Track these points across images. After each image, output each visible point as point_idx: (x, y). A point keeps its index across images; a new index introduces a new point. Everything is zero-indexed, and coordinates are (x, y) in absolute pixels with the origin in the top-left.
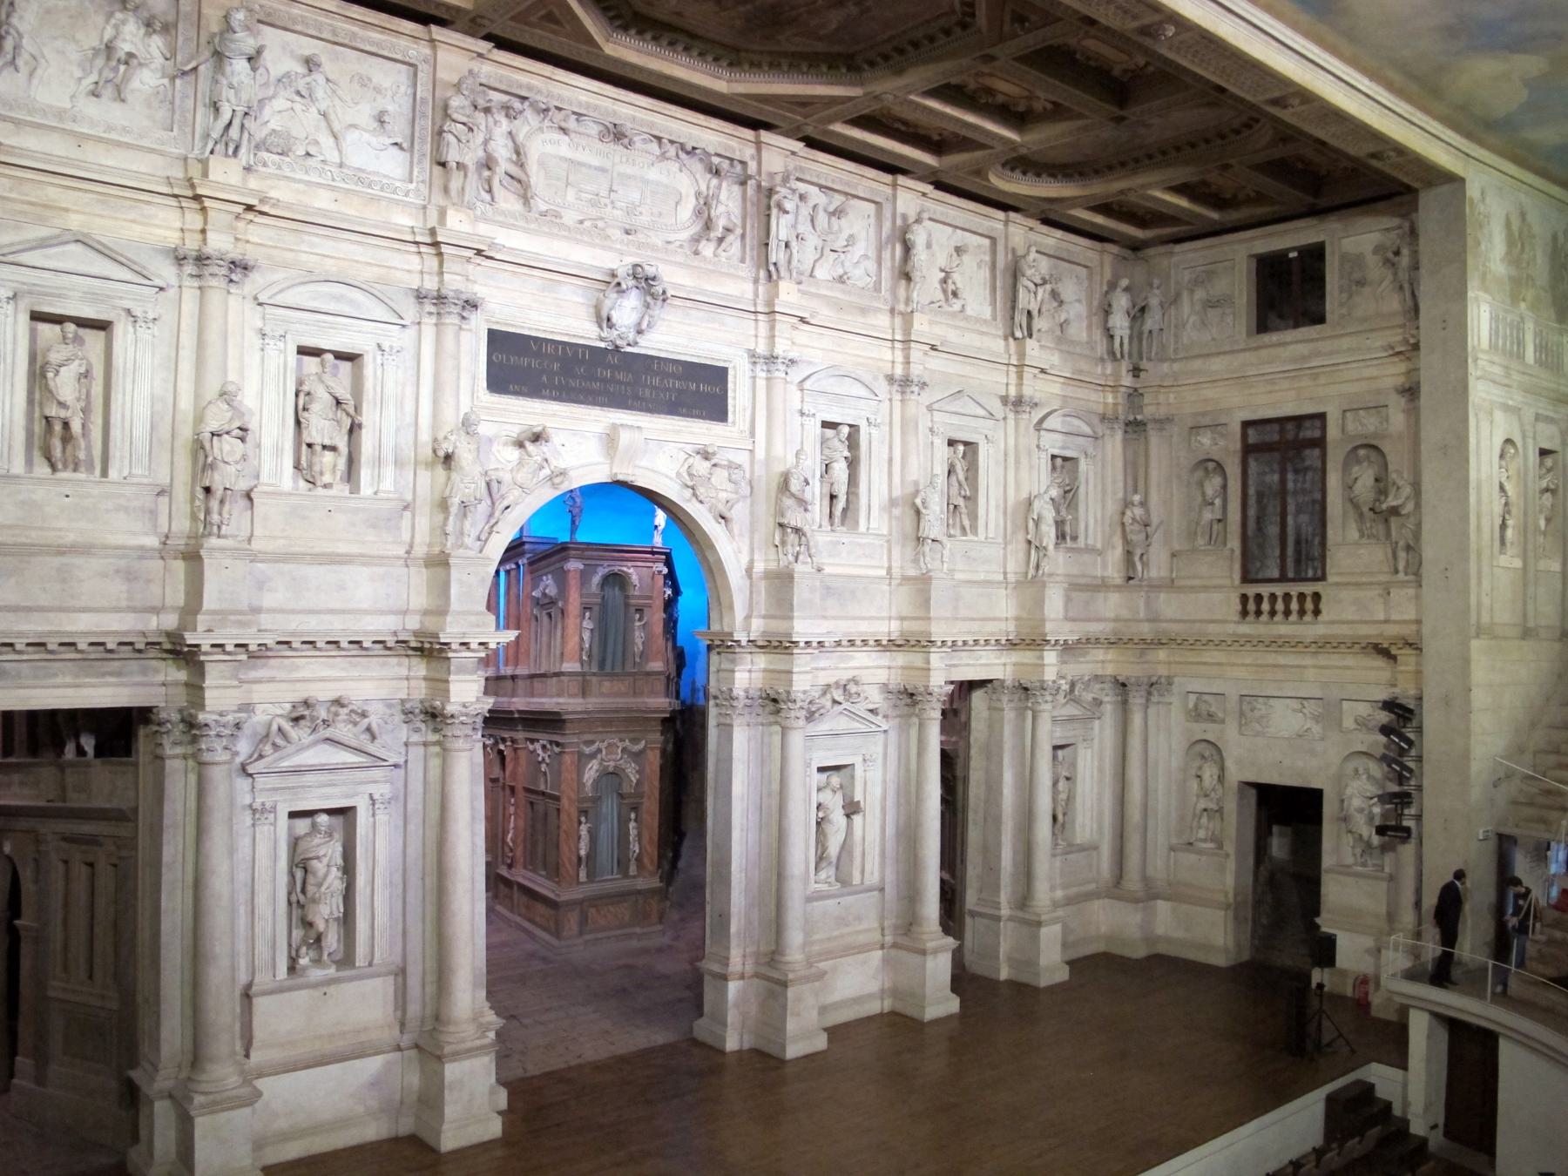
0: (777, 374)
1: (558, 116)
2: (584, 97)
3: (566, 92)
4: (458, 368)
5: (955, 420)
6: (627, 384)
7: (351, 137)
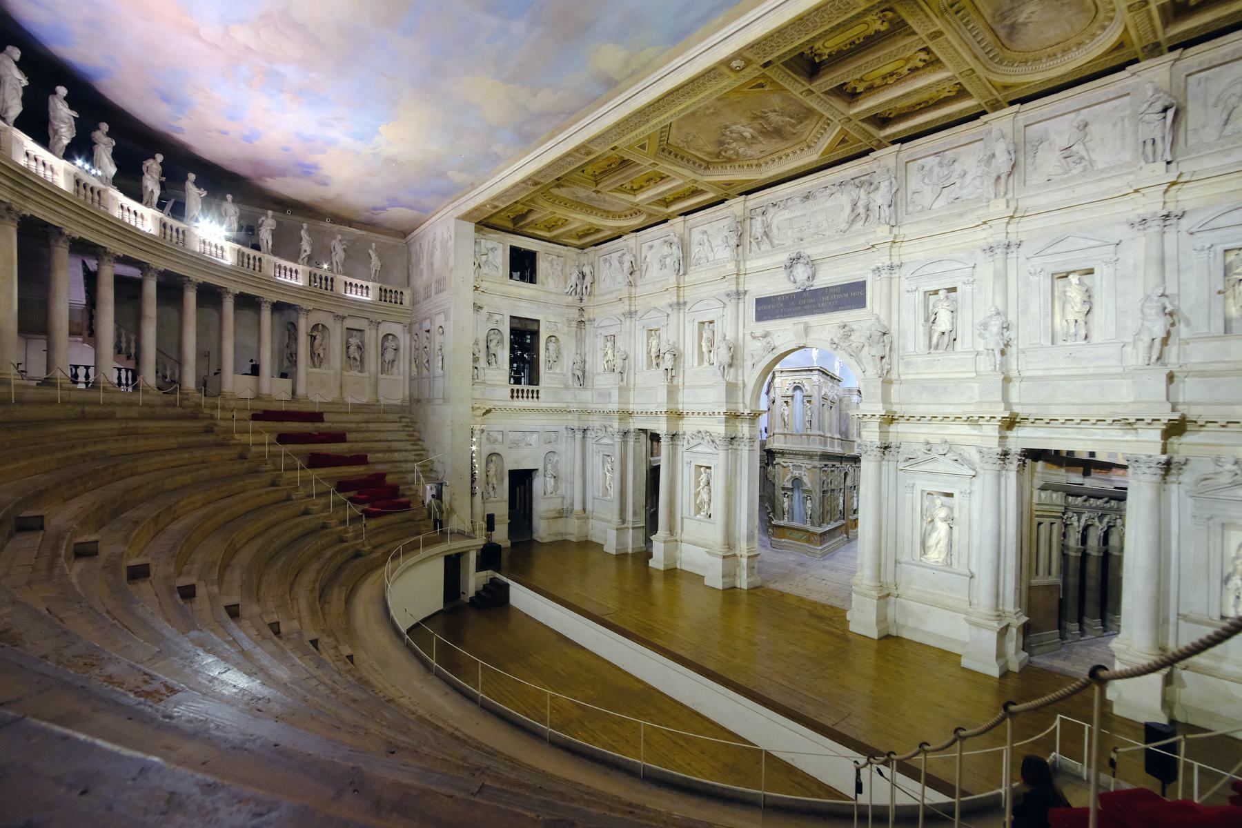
0: (882, 276)
1: (781, 204)
2: (789, 191)
3: (781, 193)
4: (738, 317)
5: (1059, 258)
6: (812, 303)
7: (715, 250)
